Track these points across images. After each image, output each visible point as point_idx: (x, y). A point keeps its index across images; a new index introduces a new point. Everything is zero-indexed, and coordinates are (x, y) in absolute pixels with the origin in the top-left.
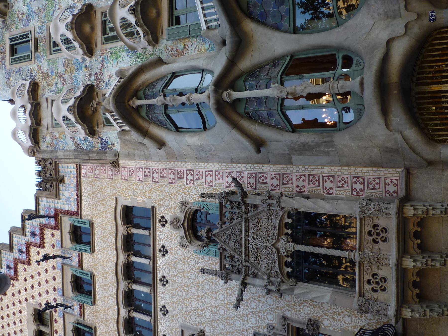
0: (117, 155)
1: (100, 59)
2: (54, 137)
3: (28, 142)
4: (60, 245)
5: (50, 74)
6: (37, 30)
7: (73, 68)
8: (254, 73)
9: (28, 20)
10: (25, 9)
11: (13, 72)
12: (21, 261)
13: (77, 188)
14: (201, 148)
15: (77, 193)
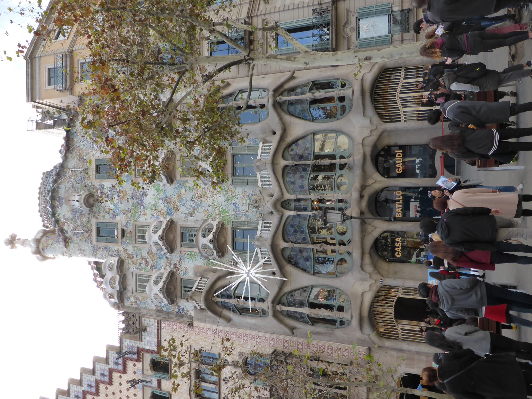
0: (191, 318)
1: (179, 256)
2: (137, 299)
3: (115, 300)
4: (141, 372)
5: (135, 256)
6: (123, 224)
7: (155, 256)
8: (291, 293)
9: (114, 216)
10: (112, 207)
11: (100, 248)
12: (103, 382)
13: (158, 336)
14: (256, 325)
15: (158, 339)
